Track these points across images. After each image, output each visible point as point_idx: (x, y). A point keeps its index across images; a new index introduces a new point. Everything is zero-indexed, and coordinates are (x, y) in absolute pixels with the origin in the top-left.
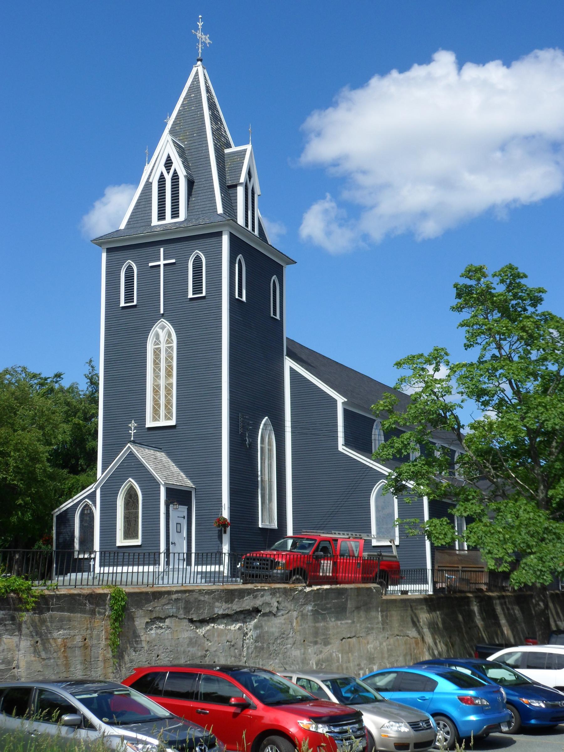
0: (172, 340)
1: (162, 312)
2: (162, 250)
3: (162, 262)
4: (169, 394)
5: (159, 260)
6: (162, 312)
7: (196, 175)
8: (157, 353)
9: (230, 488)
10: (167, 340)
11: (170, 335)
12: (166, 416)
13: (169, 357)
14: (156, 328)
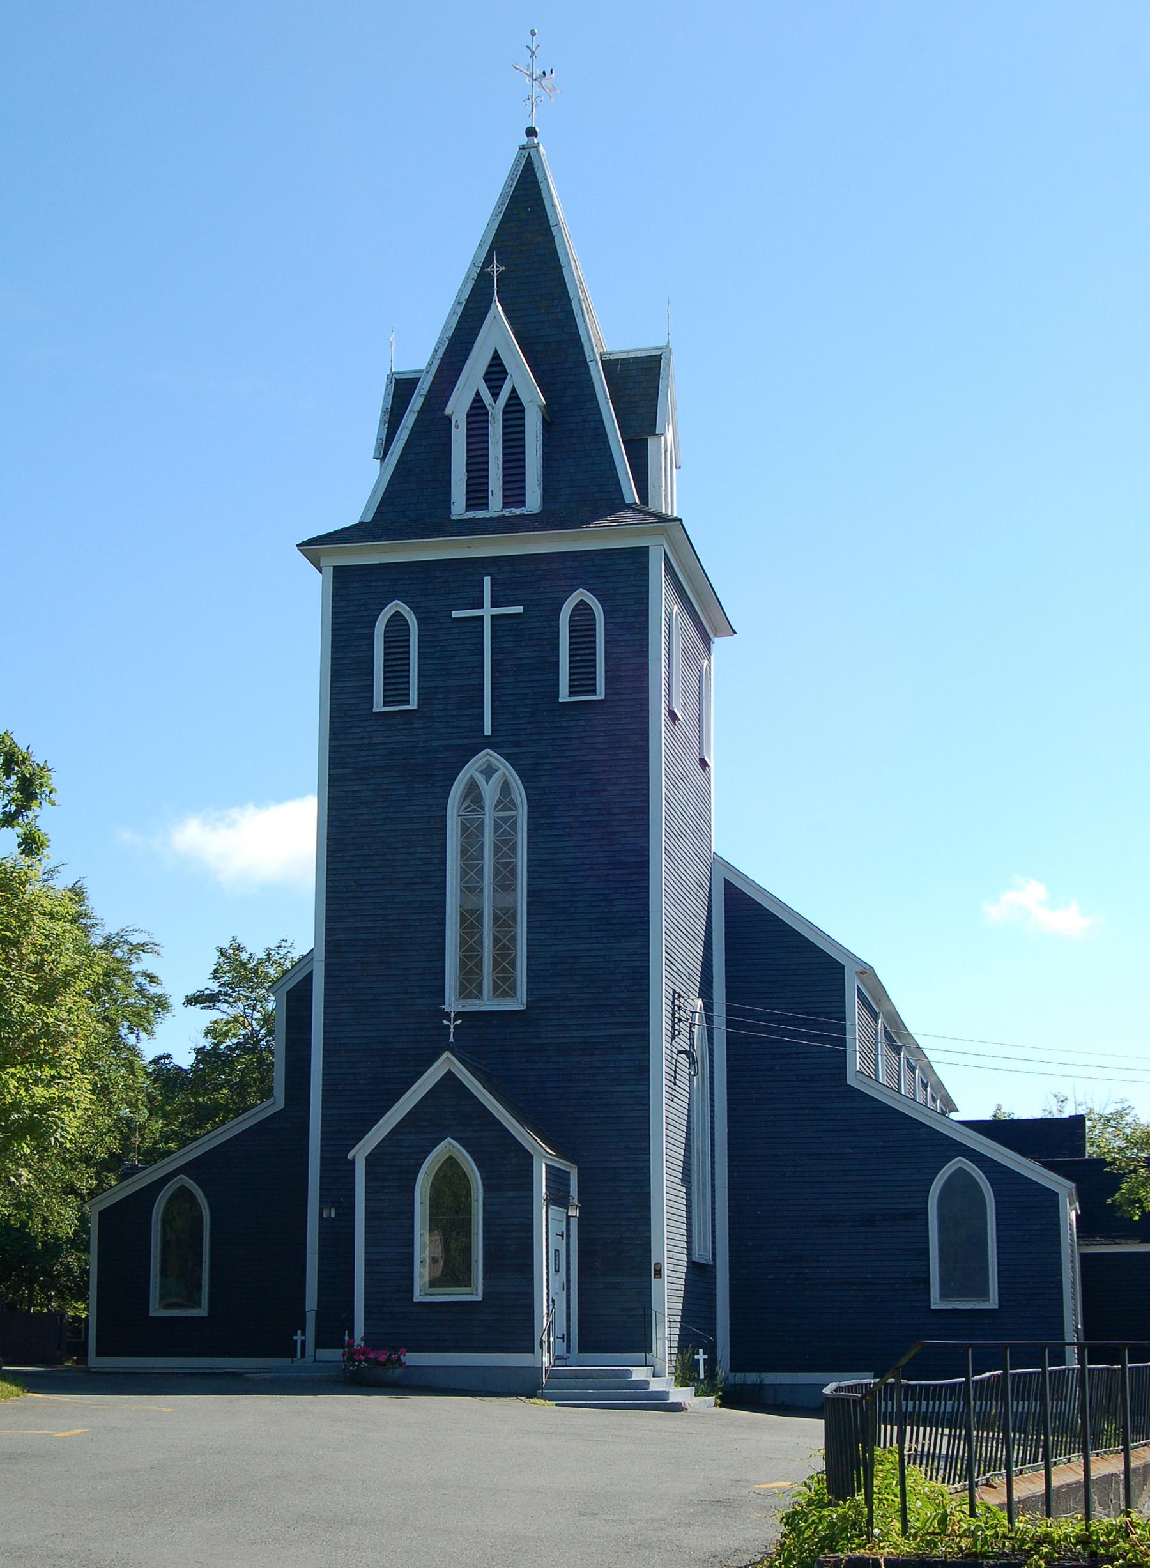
0: (512, 802)
1: (488, 731)
2: (487, 580)
3: (487, 612)
4: (504, 956)
5: (481, 606)
6: (488, 731)
7: (680, 1213)
8: (471, 832)
9: (647, 1024)
10: (499, 802)
11: (506, 789)
12: (496, 987)
13: (504, 846)
14: (471, 770)
